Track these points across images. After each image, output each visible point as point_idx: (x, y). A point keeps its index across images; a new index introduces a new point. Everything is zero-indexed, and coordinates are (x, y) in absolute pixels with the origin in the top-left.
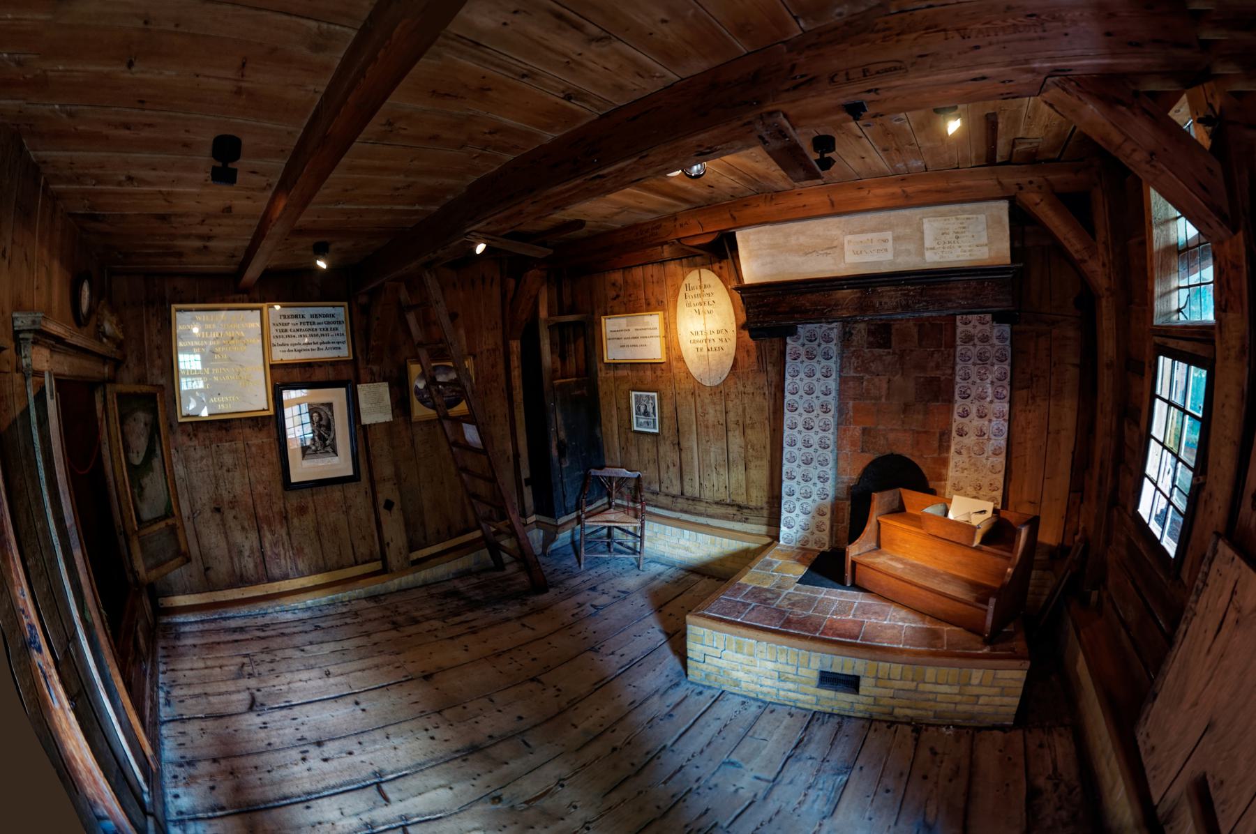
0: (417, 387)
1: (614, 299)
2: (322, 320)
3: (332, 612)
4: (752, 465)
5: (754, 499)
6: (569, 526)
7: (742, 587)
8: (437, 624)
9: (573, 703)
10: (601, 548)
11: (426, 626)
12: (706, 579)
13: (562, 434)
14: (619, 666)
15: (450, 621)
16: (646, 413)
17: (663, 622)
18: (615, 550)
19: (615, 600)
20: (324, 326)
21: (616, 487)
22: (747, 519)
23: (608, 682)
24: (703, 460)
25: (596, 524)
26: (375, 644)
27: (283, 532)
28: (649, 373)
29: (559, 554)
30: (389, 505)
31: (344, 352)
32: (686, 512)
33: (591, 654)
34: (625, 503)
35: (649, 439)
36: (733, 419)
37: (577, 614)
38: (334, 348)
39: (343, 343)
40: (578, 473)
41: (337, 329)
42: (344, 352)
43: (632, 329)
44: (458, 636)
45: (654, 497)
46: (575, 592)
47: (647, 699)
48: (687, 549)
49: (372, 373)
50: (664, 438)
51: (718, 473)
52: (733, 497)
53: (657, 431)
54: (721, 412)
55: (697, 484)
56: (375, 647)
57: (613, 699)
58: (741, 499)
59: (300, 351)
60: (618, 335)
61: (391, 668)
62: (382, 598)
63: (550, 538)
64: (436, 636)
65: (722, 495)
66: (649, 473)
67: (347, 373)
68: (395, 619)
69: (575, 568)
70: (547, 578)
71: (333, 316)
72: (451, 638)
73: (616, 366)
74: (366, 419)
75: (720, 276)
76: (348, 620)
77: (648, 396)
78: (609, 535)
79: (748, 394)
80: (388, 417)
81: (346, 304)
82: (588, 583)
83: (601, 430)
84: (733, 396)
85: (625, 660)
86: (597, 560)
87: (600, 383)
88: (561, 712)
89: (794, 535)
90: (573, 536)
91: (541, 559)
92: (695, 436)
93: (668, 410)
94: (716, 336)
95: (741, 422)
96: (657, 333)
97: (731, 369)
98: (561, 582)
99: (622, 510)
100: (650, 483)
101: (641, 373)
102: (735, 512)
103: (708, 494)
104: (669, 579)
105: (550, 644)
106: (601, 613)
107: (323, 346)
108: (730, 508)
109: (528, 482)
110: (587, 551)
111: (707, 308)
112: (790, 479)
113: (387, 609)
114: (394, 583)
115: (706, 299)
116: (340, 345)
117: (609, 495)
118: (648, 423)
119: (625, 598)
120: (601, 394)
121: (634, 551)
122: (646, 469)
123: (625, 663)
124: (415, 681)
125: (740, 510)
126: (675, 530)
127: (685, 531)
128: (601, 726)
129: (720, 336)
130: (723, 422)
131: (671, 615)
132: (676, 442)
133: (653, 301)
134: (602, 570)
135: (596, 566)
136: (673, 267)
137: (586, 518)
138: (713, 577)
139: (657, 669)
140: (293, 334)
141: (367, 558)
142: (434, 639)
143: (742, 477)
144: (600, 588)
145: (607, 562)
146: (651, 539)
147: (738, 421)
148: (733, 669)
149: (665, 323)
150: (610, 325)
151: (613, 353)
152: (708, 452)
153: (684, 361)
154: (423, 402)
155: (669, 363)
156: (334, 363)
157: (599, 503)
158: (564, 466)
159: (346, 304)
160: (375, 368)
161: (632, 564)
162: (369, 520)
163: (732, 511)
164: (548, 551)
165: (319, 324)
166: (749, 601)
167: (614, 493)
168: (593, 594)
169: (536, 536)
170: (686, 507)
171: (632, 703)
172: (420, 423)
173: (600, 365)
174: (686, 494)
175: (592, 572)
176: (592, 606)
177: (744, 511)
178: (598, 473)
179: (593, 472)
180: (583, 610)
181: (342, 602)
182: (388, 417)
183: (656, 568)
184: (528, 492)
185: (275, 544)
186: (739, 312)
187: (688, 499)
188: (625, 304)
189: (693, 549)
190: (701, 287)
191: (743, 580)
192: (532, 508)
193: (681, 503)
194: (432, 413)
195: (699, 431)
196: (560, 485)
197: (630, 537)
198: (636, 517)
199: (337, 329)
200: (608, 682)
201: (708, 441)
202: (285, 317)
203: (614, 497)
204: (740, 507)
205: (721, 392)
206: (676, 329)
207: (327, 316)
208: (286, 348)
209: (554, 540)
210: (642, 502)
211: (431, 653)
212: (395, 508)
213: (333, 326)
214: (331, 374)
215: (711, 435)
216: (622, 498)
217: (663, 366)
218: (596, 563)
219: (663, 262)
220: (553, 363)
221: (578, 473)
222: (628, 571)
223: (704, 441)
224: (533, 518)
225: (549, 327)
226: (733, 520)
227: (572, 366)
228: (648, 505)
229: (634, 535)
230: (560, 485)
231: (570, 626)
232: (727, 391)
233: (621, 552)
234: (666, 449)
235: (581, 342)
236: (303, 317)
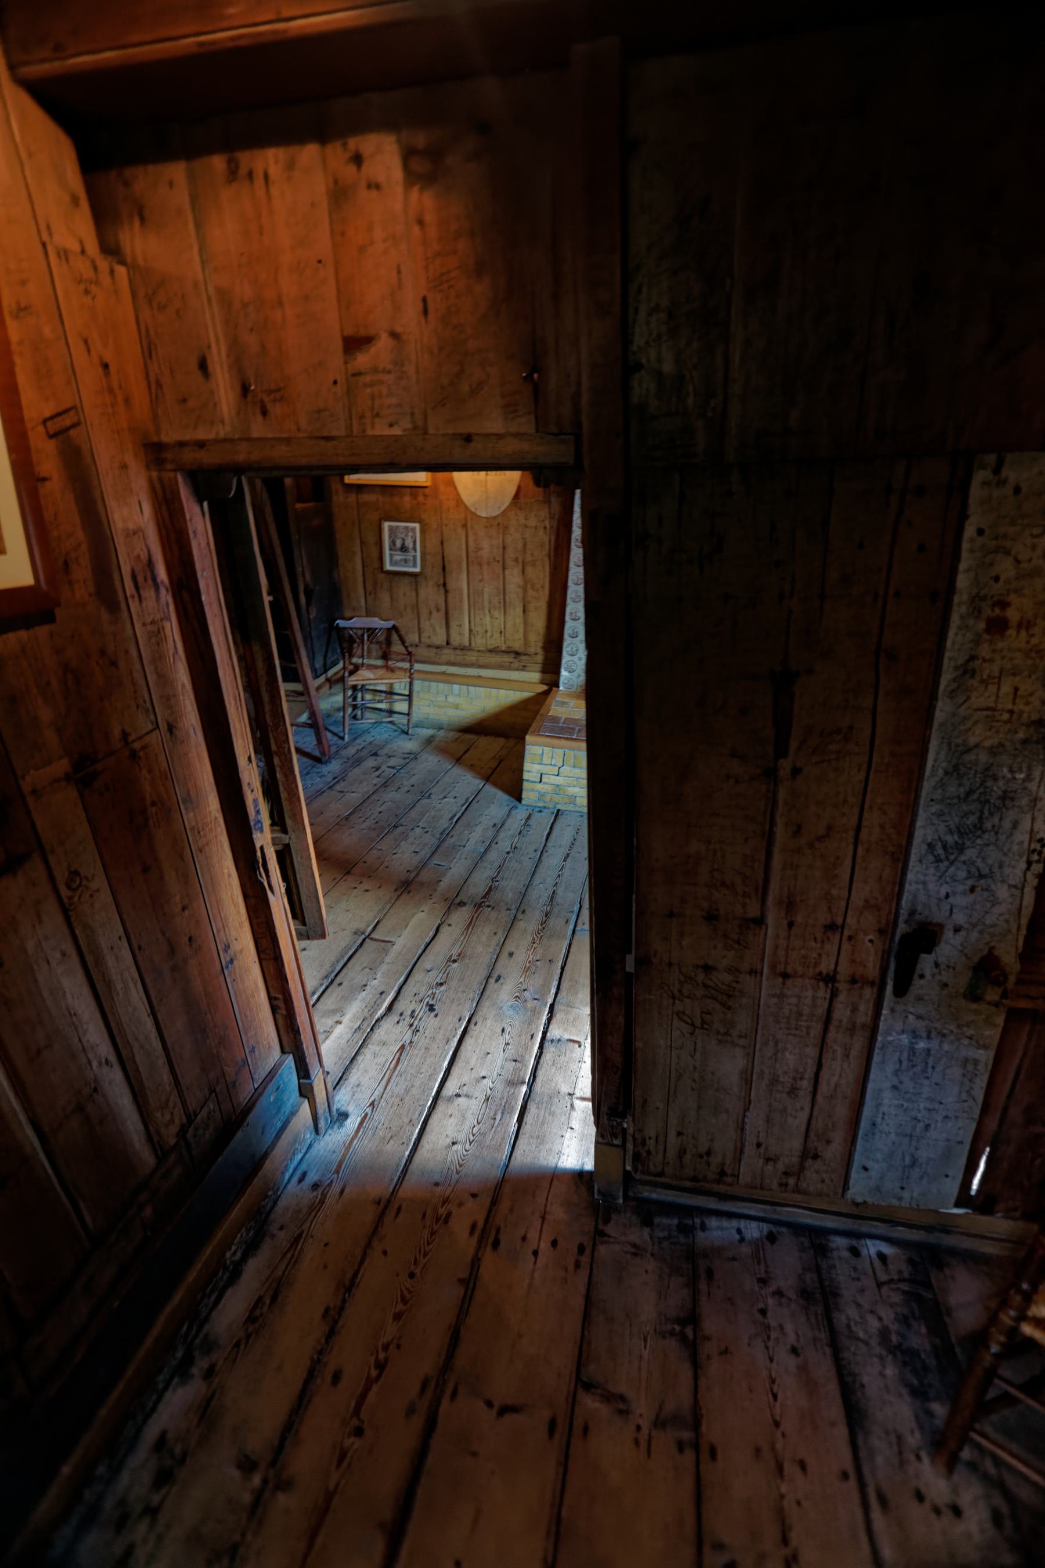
4: (531, 607)
13: (308, 575)
16: (404, 549)
22: (525, 666)
28: (407, 499)
32: (453, 664)
35: (406, 580)
48: (456, 707)
50: (426, 578)
51: (492, 617)
52: (509, 643)
53: (418, 570)
55: (467, 631)
58: (518, 645)
65: (496, 641)
77: (406, 528)
84: (512, 530)
89: (575, 680)
92: (464, 576)
93: (433, 542)
95: (520, 560)
97: (513, 499)
101: (396, 499)
102: (511, 660)
108: (506, 656)
112: (574, 620)
118: (406, 561)
125: (517, 655)
126: (441, 685)
127: (454, 686)
132: (442, 582)
143: (519, 621)
144: (381, 752)
147: (517, 558)
158: (312, 616)
163: (507, 659)
170: (452, 658)
174: (452, 641)
176: (389, 767)
187: (455, 649)
193: (448, 654)
195: (471, 569)
201: (481, 581)
204: (517, 654)
215: (485, 574)
217: (427, 491)
226: (509, 669)
234: (429, 593)
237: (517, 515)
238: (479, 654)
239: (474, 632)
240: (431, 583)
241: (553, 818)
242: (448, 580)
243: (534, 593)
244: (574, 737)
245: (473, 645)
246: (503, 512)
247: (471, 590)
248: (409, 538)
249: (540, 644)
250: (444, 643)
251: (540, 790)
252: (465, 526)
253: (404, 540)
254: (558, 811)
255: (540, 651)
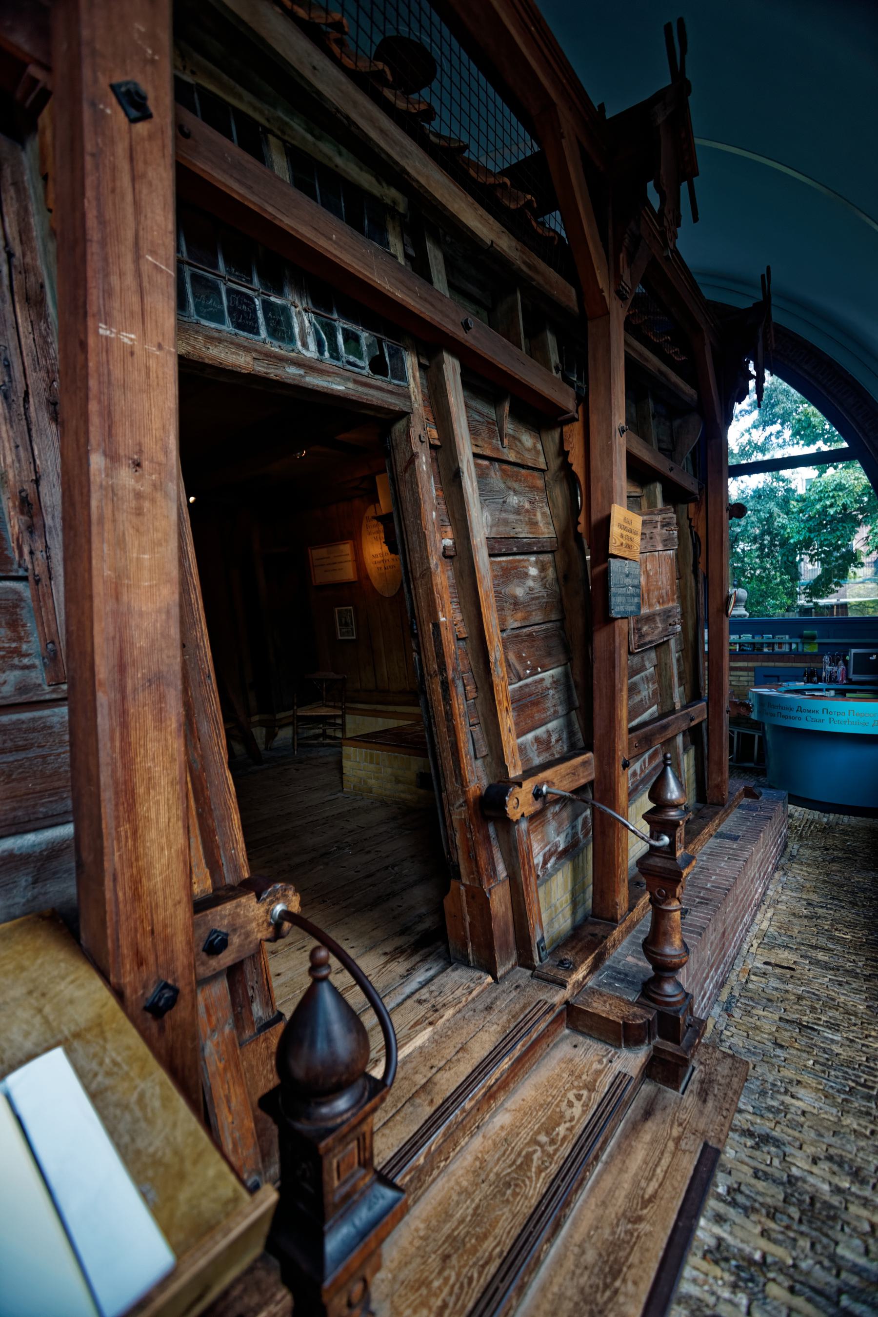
16: (346, 624)
63: (271, 736)
77: (346, 610)
96: (349, 558)
150: (317, 554)
151: (320, 577)
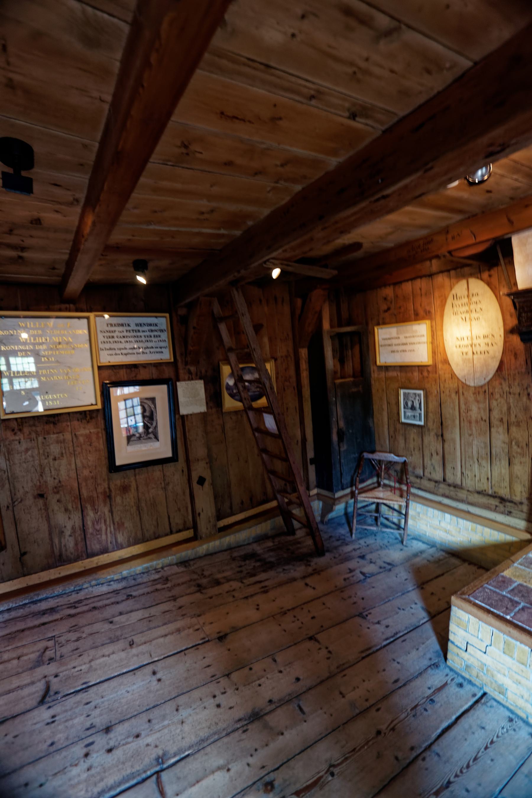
0: (228, 384)
1: (386, 311)
2: (146, 328)
3: (145, 580)
4: (516, 461)
5: (518, 494)
6: (344, 500)
7: (506, 582)
8: (235, 584)
9: (342, 669)
10: (369, 521)
11: (226, 587)
12: (466, 564)
13: (342, 424)
14: (384, 637)
15: (247, 581)
16: (413, 408)
17: (425, 599)
18: (382, 524)
19: (381, 570)
20: (148, 333)
21: (385, 469)
22: (510, 512)
23: (374, 652)
24: (465, 451)
25: (367, 499)
26: (180, 608)
27: (106, 510)
28: (416, 374)
29: (334, 523)
30: (201, 481)
31: (166, 356)
33: (358, 620)
34: (392, 484)
36: (497, 417)
37: (348, 578)
38: (157, 352)
39: (165, 348)
40: (353, 456)
41: (160, 336)
42: (166, 356)
43: (402, 337)
44: (252, 596)
45: (418, 481)
46: (347, 558)
47: (410, 681)
48: (447, 532)
49: (190, 372)
50: (429, 430)
51: (480, 465)
52: (496, 489)
53: (422, 423)
54: (485, 410)
56: (180, 610)
57: (378, 672)
58: (504, 492)
59: (126, 354)
60: (389, 342)
61: (191, 630)
62: (192, 563)
63: (328, 508)
64: (234, 597)
65: (484, 486)
66: (413, 459)
67: (168, 373)
68: (199, 582)
69: (348, 537)
70: (325, 543)
71: (156, 325)
72: (246, 598)
73: (387, 368)
74: (184, 411)
75: (489, 284)
76: (159, 586)
77: (415, 394)
78: (377, 510)
79: (514, 394)
80: (202, 408)
81: (167, 315)
82: (358, 552)
83: (373, 421)
84: (497, 396)
85: (389, 632)
86: (366, 531)
87: (373, 382)
88: (331, 676)
90: (346, 508)
91: (321, 527)
93: (433, 405)
94: (482, 341)
95: (505, 420)
96: (424, 339)
97: (497, 371)
98: (336, 548)
99: (389, 489)
100: (414, 468)
101: (409, 374)
103: (469, 483)
104: (430, 558)
105: (324, 604)
106: (368, 580)
107: (148, 351)
108: (492, 499)
109: (312, 461)
110: (359, 523)
111: (473, 315)
113: (194, 572)
114: (203, 548)
115: (473, 307)
116: (163, 350)
117: (378, 476)
118: (414, 416)
119: (390, 570)
120: (374, 391)
121: (399, 527)
122: (412, 455)
123: (389, 634)
124: (210, 643)
126: (436, 512)
128: (367, 700)
129: (487, 340)
130: (486, 417)
131: (432, 594)
133: (421, 313)
134: (370, 541)
135: (365, 537)
136: (440, 279)
137: (359, 493)
138: (475, 564)
139: (420, 649)
140: (119, 340)
141: (181, 527)
142: (231, 599)
143: (505, 471)
144: (368, 557)
145: (375, 534)
146: (414, 519)
148: (499, 672)
149: (432, 331)
152: (470, 445)
153: (449, 364)
154: (232, 396)
155: (435, 366)
156: (158, 365)
157: (369, 482)
159: (167, 315)
160: (193, 369)
161: (396, 539)
162: (184, 493)
163: (494, 502)
164: (326, 519)
165: (143, 331)
166: (516, 599)
167: (383, 473)
168: (362, 562)
169: (317, 506)
170: (447, 492)
171: (396, 681)
172: (229, 413)
173: (373, 368)
175: (362, 542)
177: (508, 504)
178: (370, 456)
179: (366, 455)
180: (353, 576)
181: (155, 569)
182: (202, 408)
183: (418, 546)
184: (312, 470)
185: (97, 522)
186: (508, 317)
187: (449, 485)
188: (395, 315)
189: (454, 532)
190: (468, 296)
191: (507, 573)
192: (315, 483)
194: (239, 405)
195: (462, 424)
196: (338, 466)
197: (396, 514)
198: (401, 496)
199: (160, 336)
200: (374, 652)
201: (470, 435)
202: (111, 325)
203: (383, 477)
204: (503, 500)
205: (485, 392)
206: (442, 335)
207: (150, 325)
208: (113, 352)
209: (331, 510)
210: (407, 484)
211: (228, 613)
212: (206, 484)
213: (156, 333)
214: (154, 374)
215: (474, 429)
216: (389, 479)
218: (365, 534)
219: (431, 276)
220: (334, 366)
221: (353, 456)
222: (392, 545)
223: (467, 435)
224: (314, 491)
225: (331, 337)
227: (349, 368)
228: (412, 487)
229: (400, 512)
230: (338, 466)
231: (342, 590)
232: (491, 390)
233: (386, 526)
235: (357, 349)
236: (129, 325)
237: (501, 384)
238: (469, 493)
239: (465, 475)
240: (432, 434)
241: (470, 704)
242: (444, 432)
243: (519, 450)
244: (508, 617)
245: (464, 484)
246: (488, 383)
247: (463, 442)
248: (417, 401)
249: (525, 495)
250: (442, 479)
251: (465, 658)
252: (457, 392)
253: (413, 402)
254: (485, 694)
255: (525, 502)
